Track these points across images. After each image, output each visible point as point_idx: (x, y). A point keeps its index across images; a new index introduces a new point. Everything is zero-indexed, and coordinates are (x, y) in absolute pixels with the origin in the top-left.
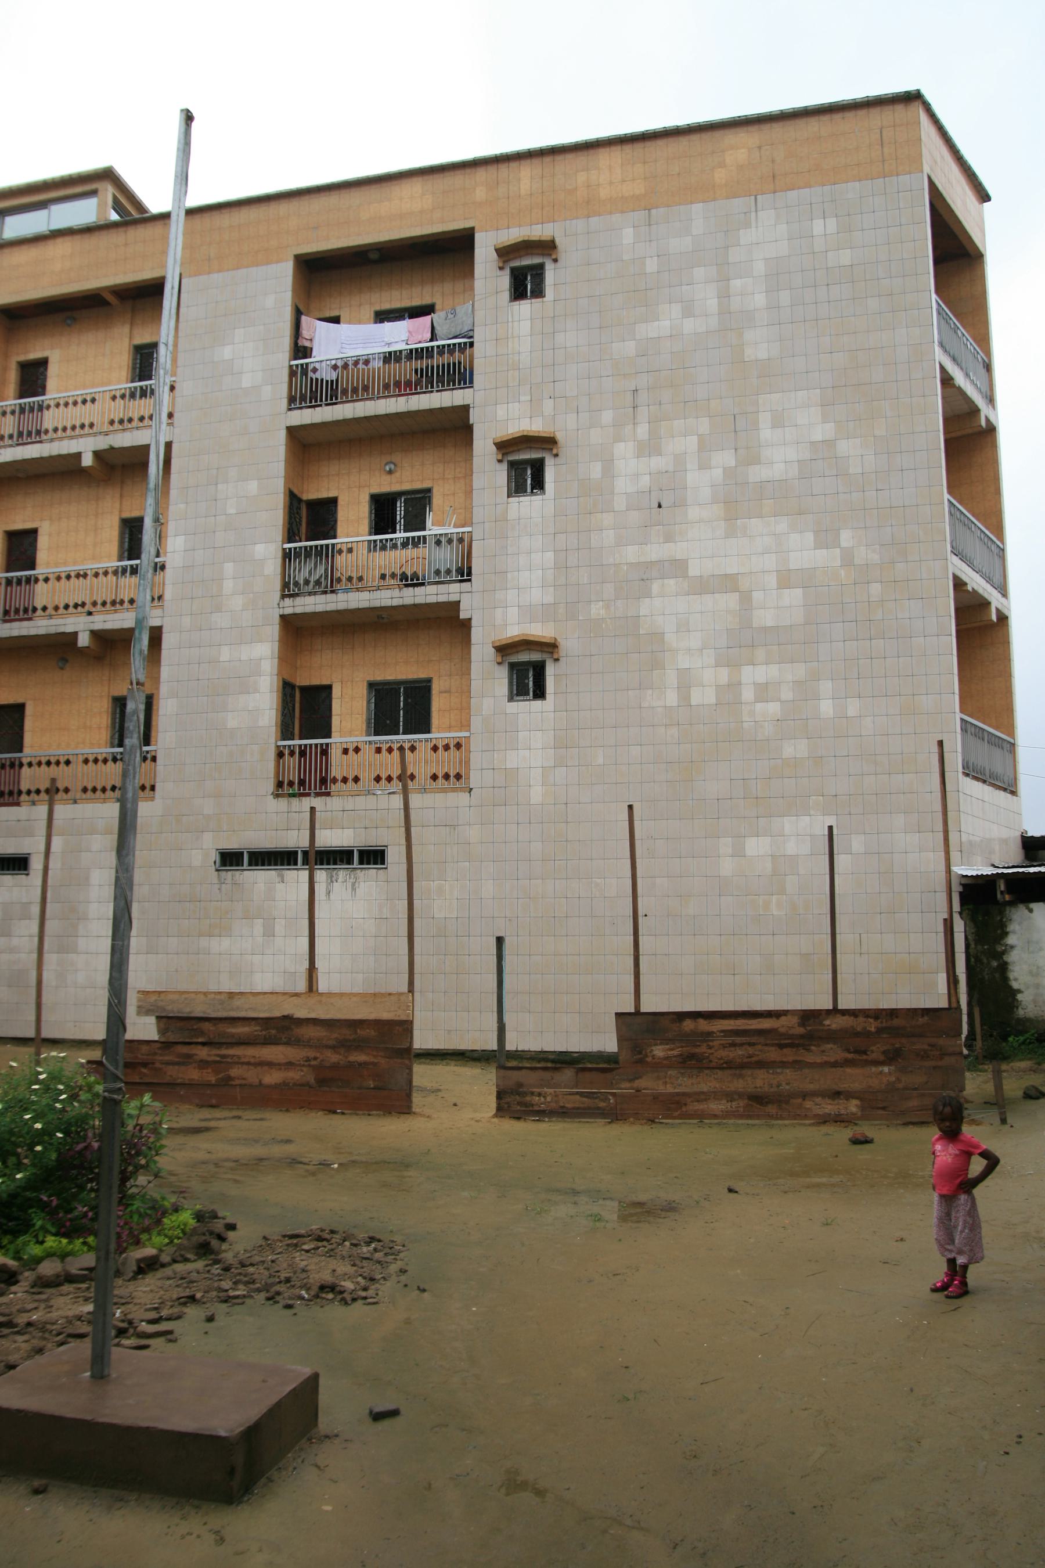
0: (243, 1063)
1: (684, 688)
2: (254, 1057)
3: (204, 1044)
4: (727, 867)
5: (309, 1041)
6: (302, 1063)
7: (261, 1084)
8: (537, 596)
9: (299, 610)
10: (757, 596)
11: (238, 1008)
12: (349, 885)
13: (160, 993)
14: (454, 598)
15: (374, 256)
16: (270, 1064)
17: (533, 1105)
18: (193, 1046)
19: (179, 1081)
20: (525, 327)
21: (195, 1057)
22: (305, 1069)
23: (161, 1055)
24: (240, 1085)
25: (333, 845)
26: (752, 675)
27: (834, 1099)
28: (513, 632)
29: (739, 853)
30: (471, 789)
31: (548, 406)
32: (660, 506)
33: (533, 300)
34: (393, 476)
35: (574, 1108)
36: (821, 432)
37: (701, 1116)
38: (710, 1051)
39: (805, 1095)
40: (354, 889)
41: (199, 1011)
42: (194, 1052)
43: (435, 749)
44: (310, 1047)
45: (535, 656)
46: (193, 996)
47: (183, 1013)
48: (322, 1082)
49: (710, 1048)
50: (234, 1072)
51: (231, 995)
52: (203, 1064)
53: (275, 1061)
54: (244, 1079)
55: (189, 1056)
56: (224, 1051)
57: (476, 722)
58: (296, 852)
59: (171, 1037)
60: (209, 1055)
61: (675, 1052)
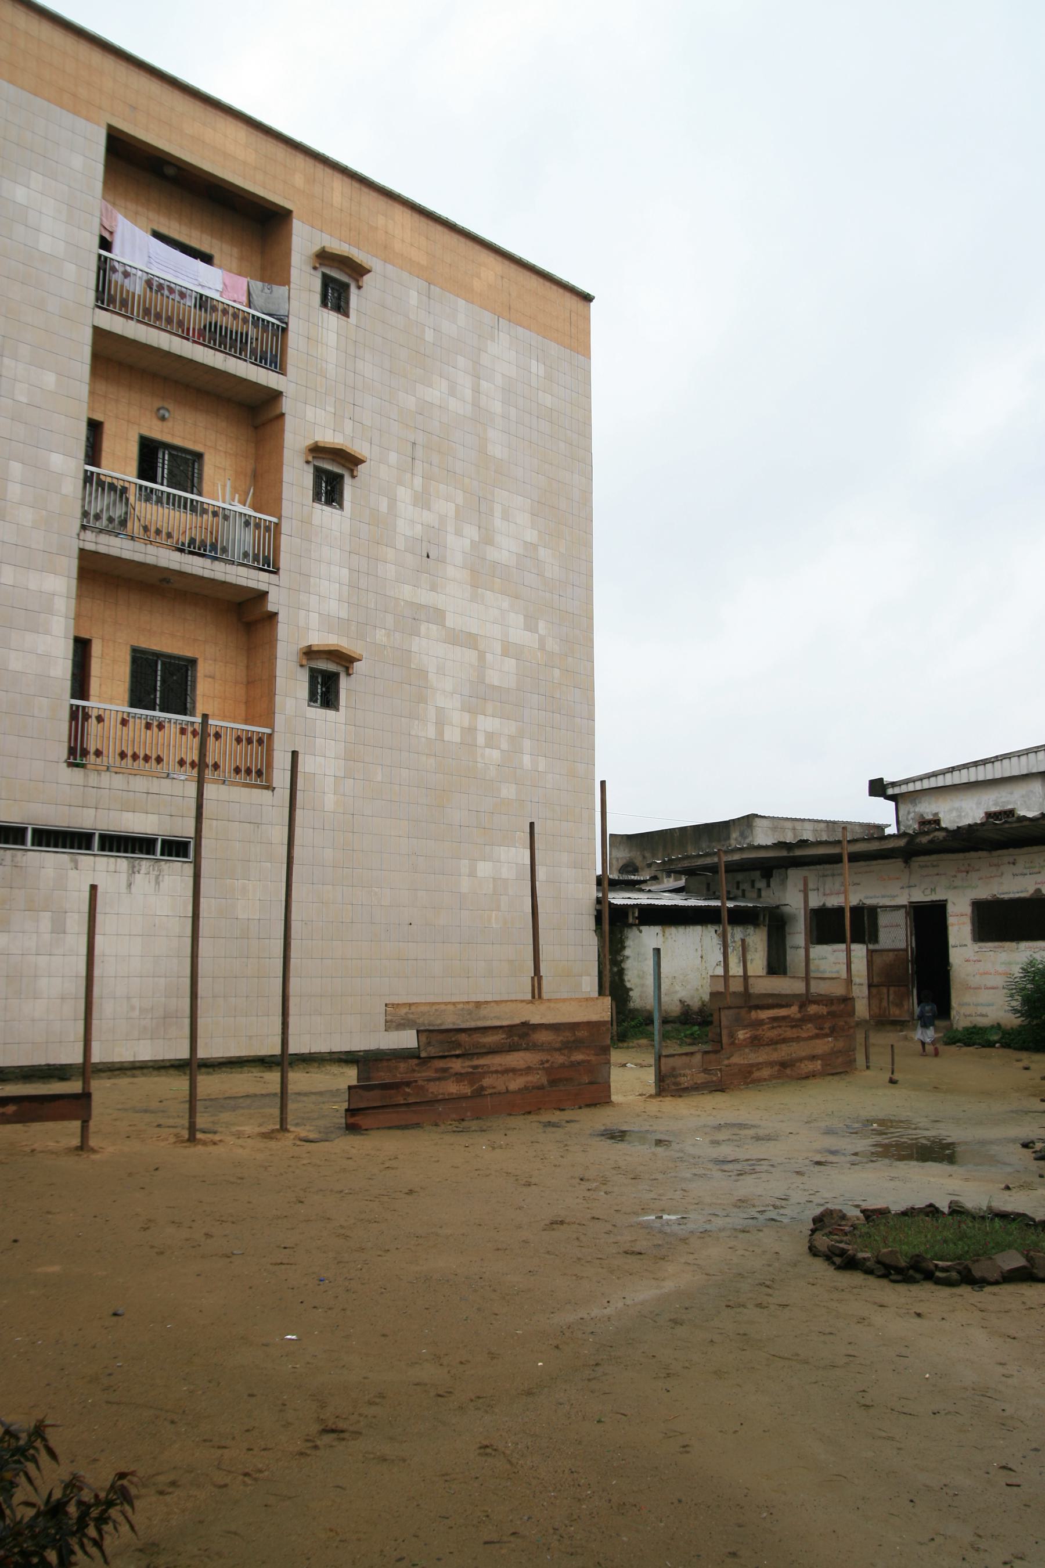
0: (492, 1072)
1: (440, 724)
2: (501, 1065)
3: (457, 1056)
4: (465, 885)
5: (542, 1046)
6: (538, 1066)
7: (507, 1091)
8: (336, 608)
9: (102, 549)
10: (489, 657)
11: (485, 1018)
12: (153, 877)
13: (410, 1005)
14: (263, 587)
15: (170, 171)
16: (513, 1070)
17: (680, 1084)
18: (448, 1059)
19: (440, 1097)
20: (332, 338)
21: (451, 1070)
22: (540, 1072)
23: (419, 1072)
24: (491, 1094)
25: (136, 831)
26: (486, 723)
27: (811, 1061)
28: (319, 639)
29: (472, 874)
30: (274, 788)
31: (348, 426)
32: (428, 557)
33: (331, 312)
34: (165, 424)
35: (702, 1083)
36: (531, 536)
37: (759, 1081)
38: (763, 1033)
39: (801, 1060)
40: (157, 883)
41: (449, 1021)
42: (450, 1065)
43: (239, 740)
44: (543, 1050)
45: (331, 667)
46: (443, 1007)
47: (434, 1025)
48: (553, 1082)
49: (763, 1031)
50: (486, 1082)
51: (478, 1004)
52: (460, 1077)
53: (519, 1067)
54: (494, 1088)
55: (445, 1070)
56: (476, 1062)
57: (279, 720)
58: (155, 840)
59: (433, 1051)
60: (463, 1067)
61: (748, 1035)
